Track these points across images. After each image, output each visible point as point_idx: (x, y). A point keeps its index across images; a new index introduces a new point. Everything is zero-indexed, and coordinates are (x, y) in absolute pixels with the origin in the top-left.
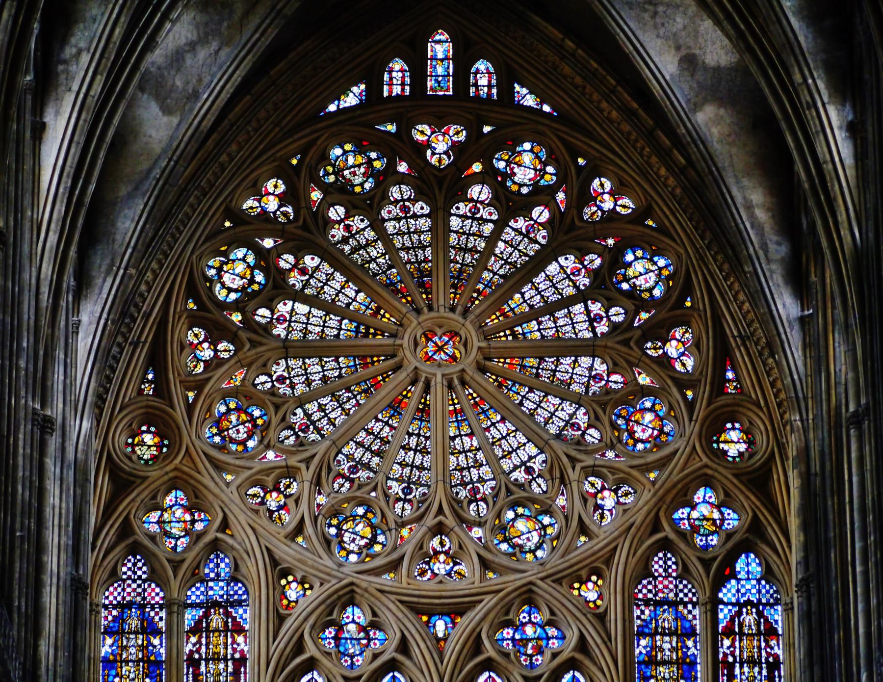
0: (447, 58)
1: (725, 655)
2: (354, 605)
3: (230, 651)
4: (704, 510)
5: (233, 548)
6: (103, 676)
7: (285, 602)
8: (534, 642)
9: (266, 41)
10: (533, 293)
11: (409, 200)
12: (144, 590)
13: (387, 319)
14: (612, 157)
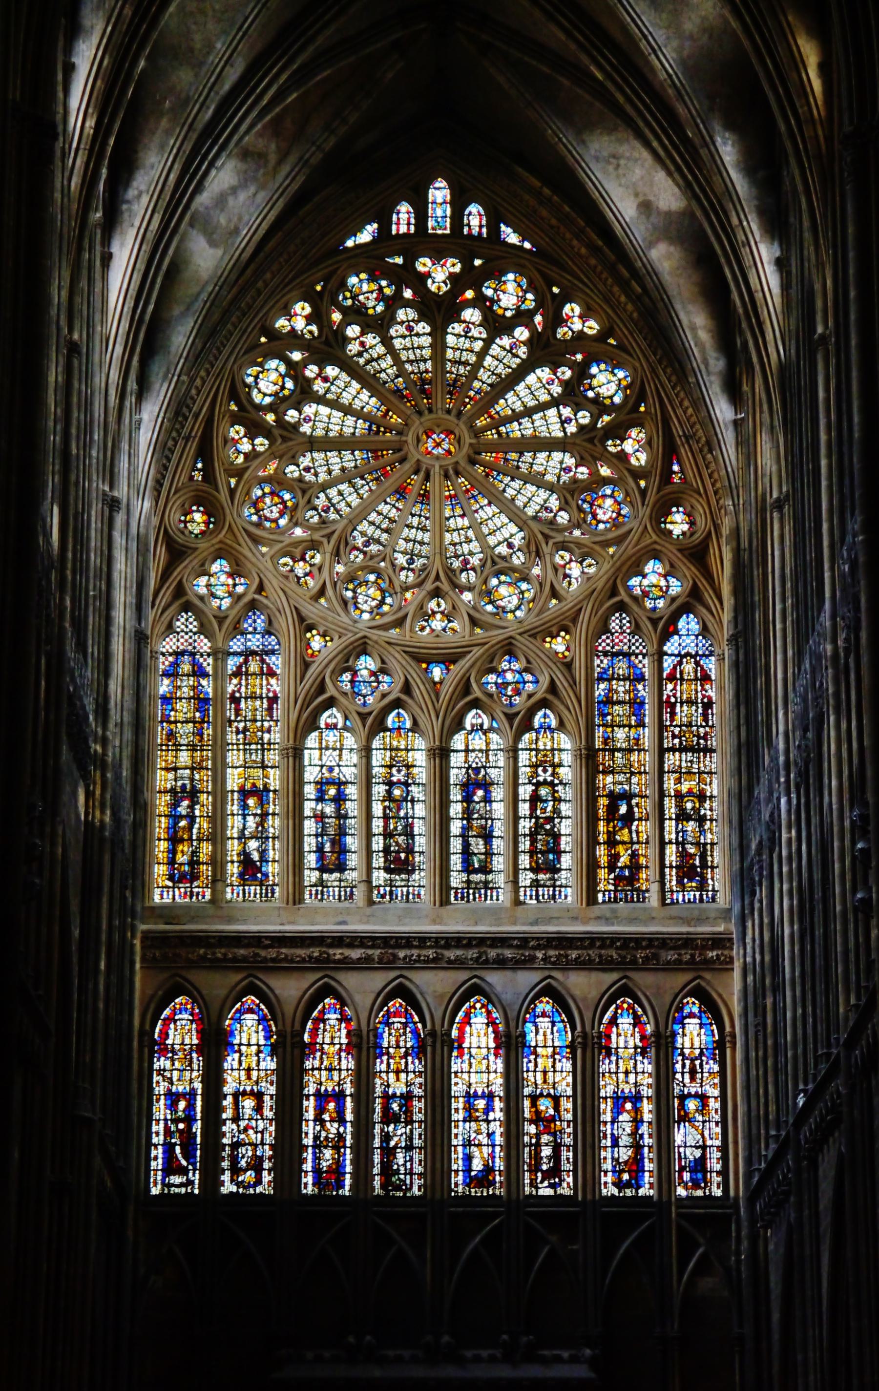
0: (445, 202)
2: (366, 654)
4: (653, 579)
5: (267, 607)
7: (310, 651)
8: (513, 686)
9: (295, 186)
10: (515, 398)
11: (413, 321)
12: (195, 641)
13: (395, 419)
14: (580, 285)
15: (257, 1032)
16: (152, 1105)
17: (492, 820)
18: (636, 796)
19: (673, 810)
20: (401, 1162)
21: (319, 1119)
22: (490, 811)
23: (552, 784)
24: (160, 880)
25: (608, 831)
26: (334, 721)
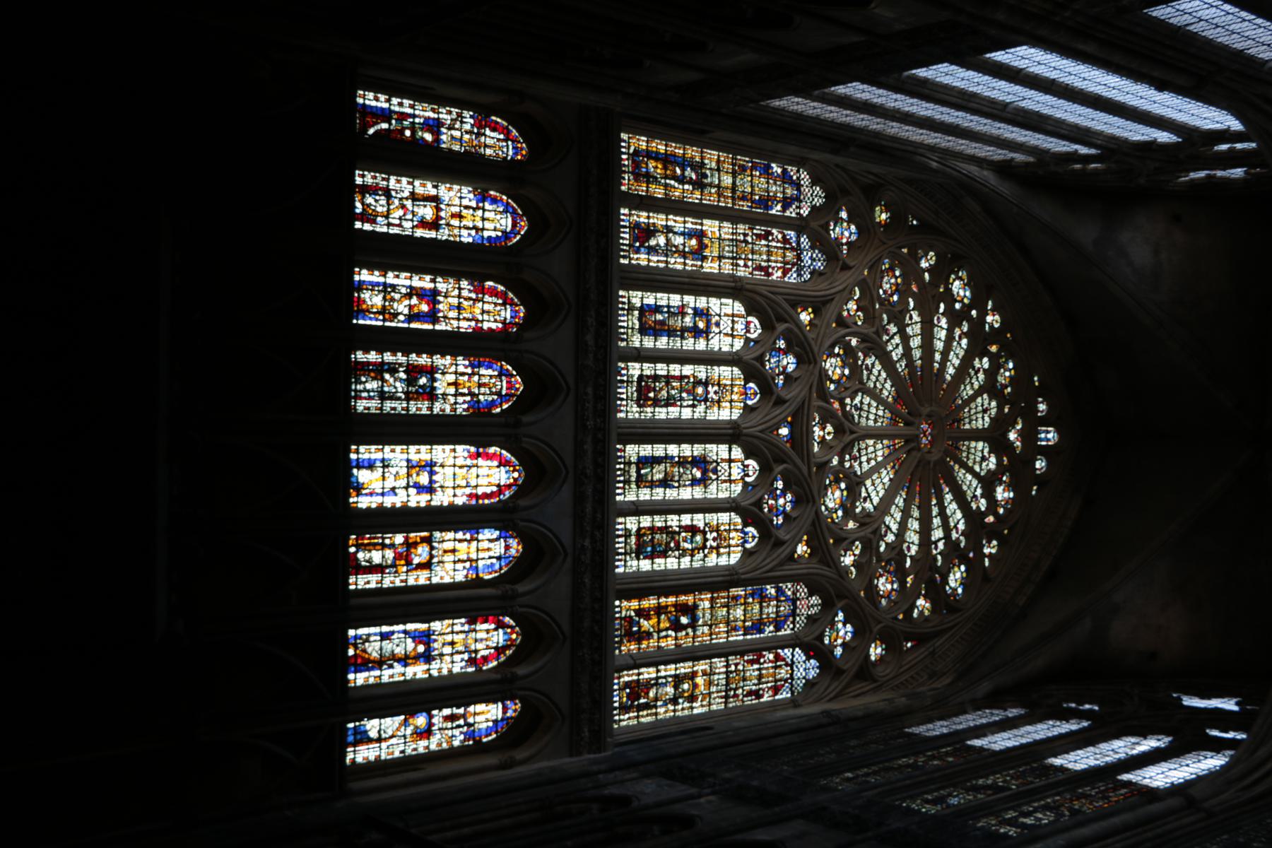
0: (1048, 440)
1: (764, 656)
2: (798, 363)
3: (773, 264)
6: (760, 163)
10: (949, 500)
12: (806, 202)
15: (495, 229)
16: (430, 104)
17: (678, 487)
18: (694, 631)
19: (683, 671)
20: (369, 386)
21: (412, 292)
22: (685, 486)
23: (704, 547)
24: (634, 141)
25: (667, 606)
26: (752, 331)
